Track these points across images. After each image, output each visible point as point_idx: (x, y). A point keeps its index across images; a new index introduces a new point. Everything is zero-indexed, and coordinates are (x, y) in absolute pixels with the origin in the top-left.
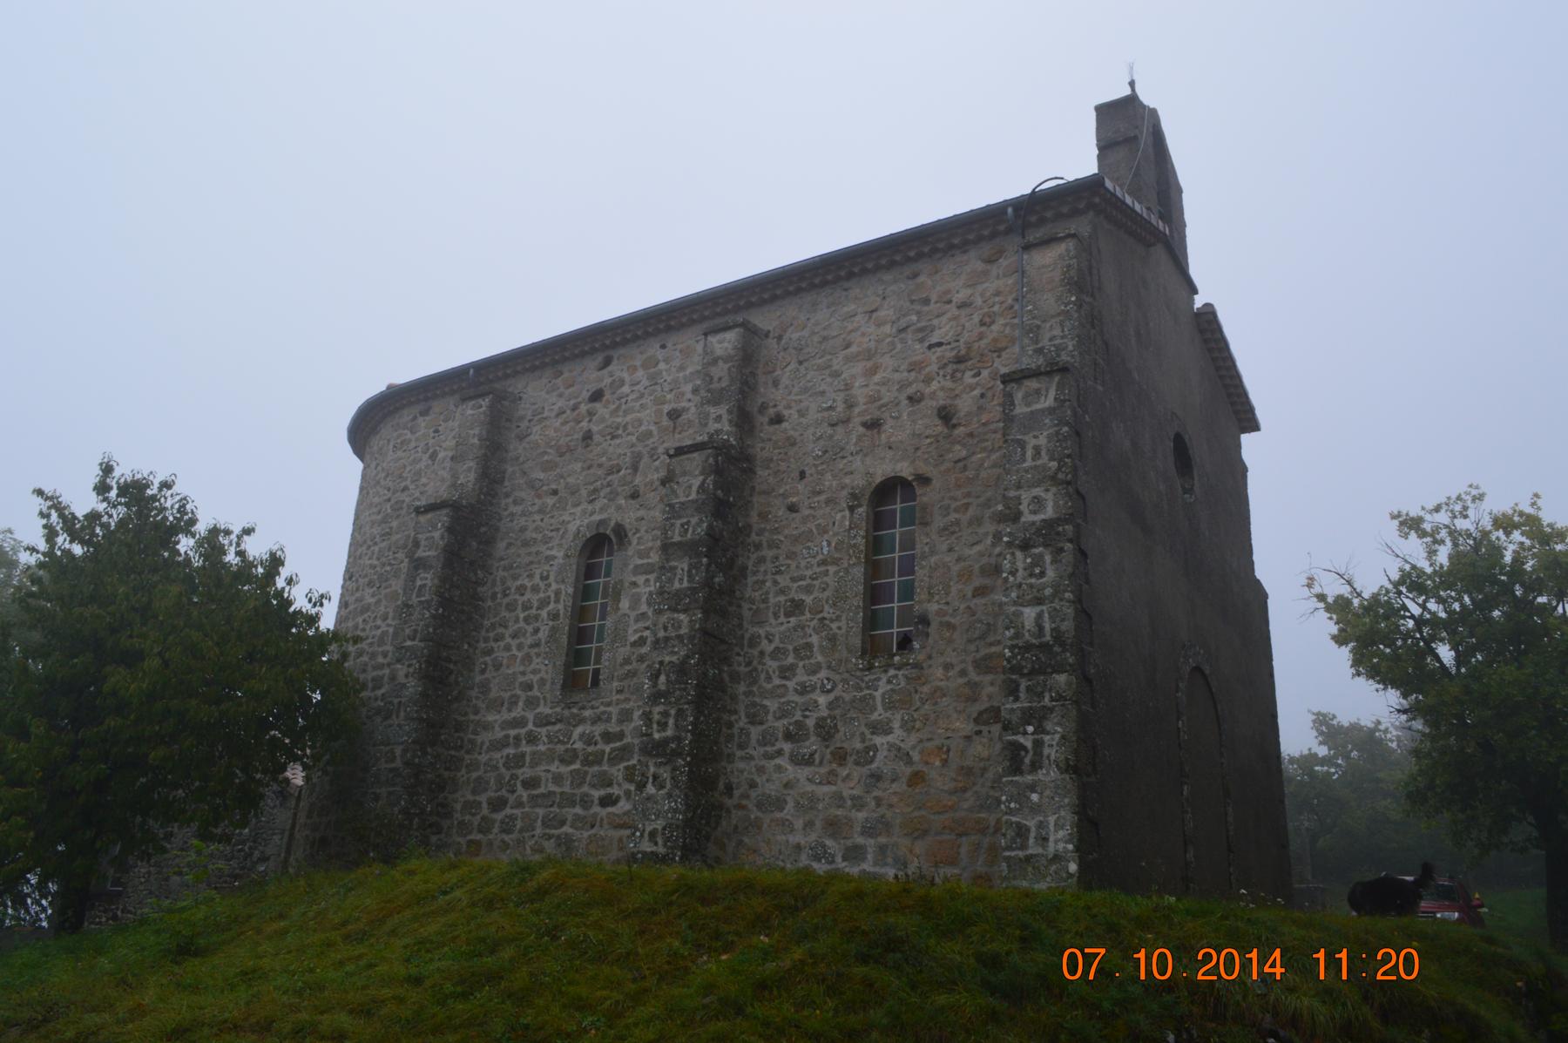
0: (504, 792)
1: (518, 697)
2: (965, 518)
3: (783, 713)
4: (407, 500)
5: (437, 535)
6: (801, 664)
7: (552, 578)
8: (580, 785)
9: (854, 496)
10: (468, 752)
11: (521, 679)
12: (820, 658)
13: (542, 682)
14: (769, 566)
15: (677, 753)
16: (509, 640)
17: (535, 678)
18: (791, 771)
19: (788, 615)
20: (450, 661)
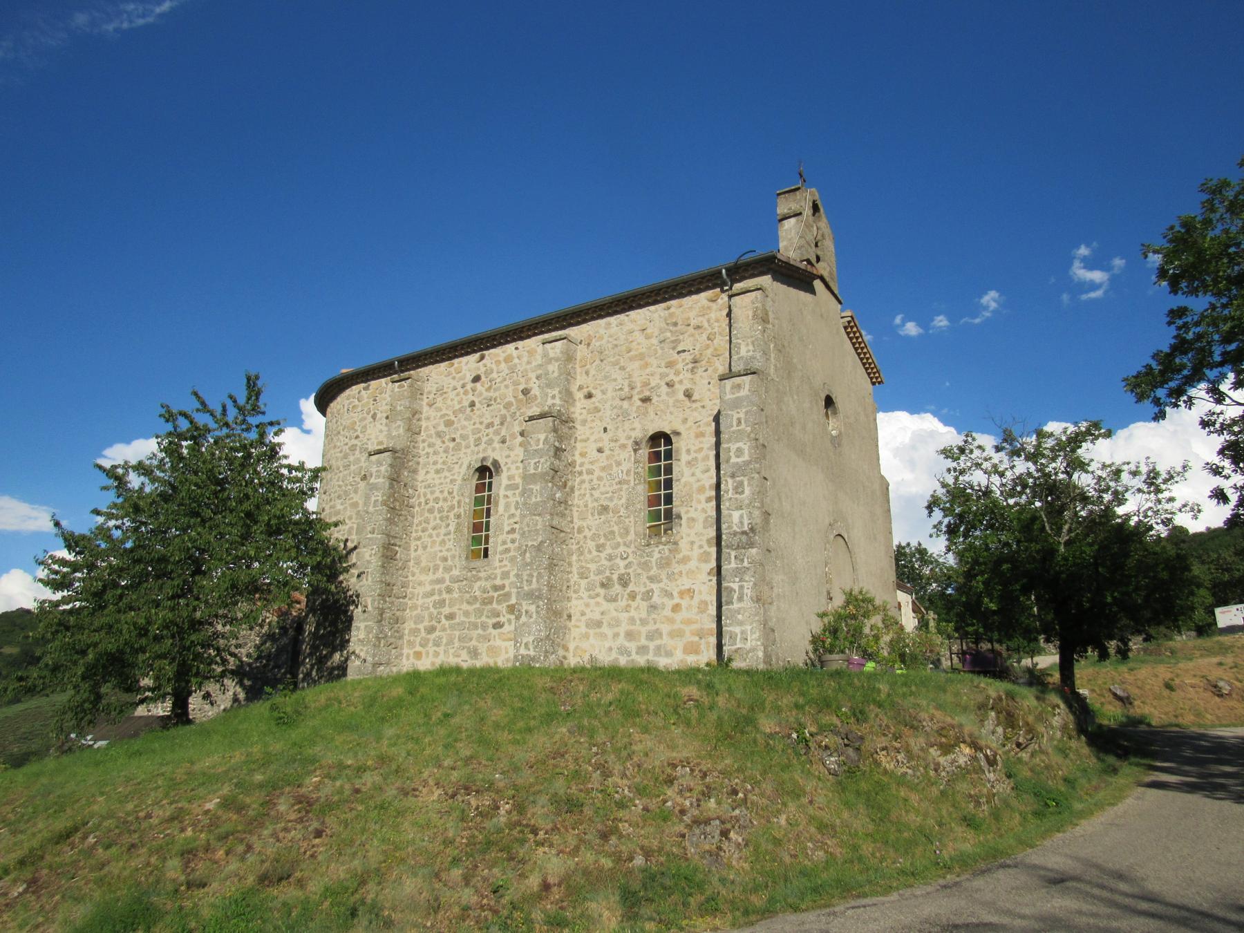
0: (434, 623)
1: (439, 565)
2: (700, 456)
3: (599, 572)
4: (359, 444)
5: (383, 468)
6: (608, 543)
7: (455, 493)
8: (480, 617)
9: (636, 443)
10: (410, 599)
11: (440, 554)
12: (619, 540)
13: (453, 557)
14: (586, 485)
15: (539, 597)
16: (431, 531)
17: (449, 554)
18: (606, 606)
19: (600, 514)
20: (396, 545)
